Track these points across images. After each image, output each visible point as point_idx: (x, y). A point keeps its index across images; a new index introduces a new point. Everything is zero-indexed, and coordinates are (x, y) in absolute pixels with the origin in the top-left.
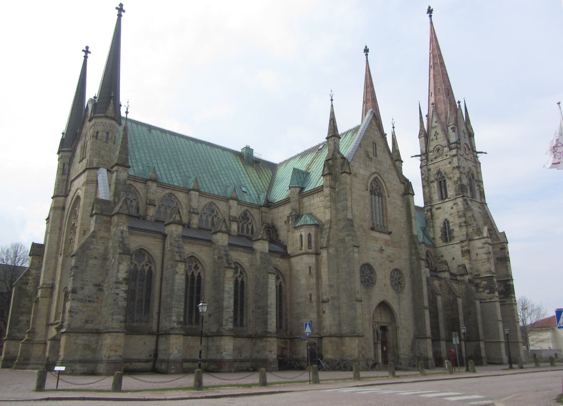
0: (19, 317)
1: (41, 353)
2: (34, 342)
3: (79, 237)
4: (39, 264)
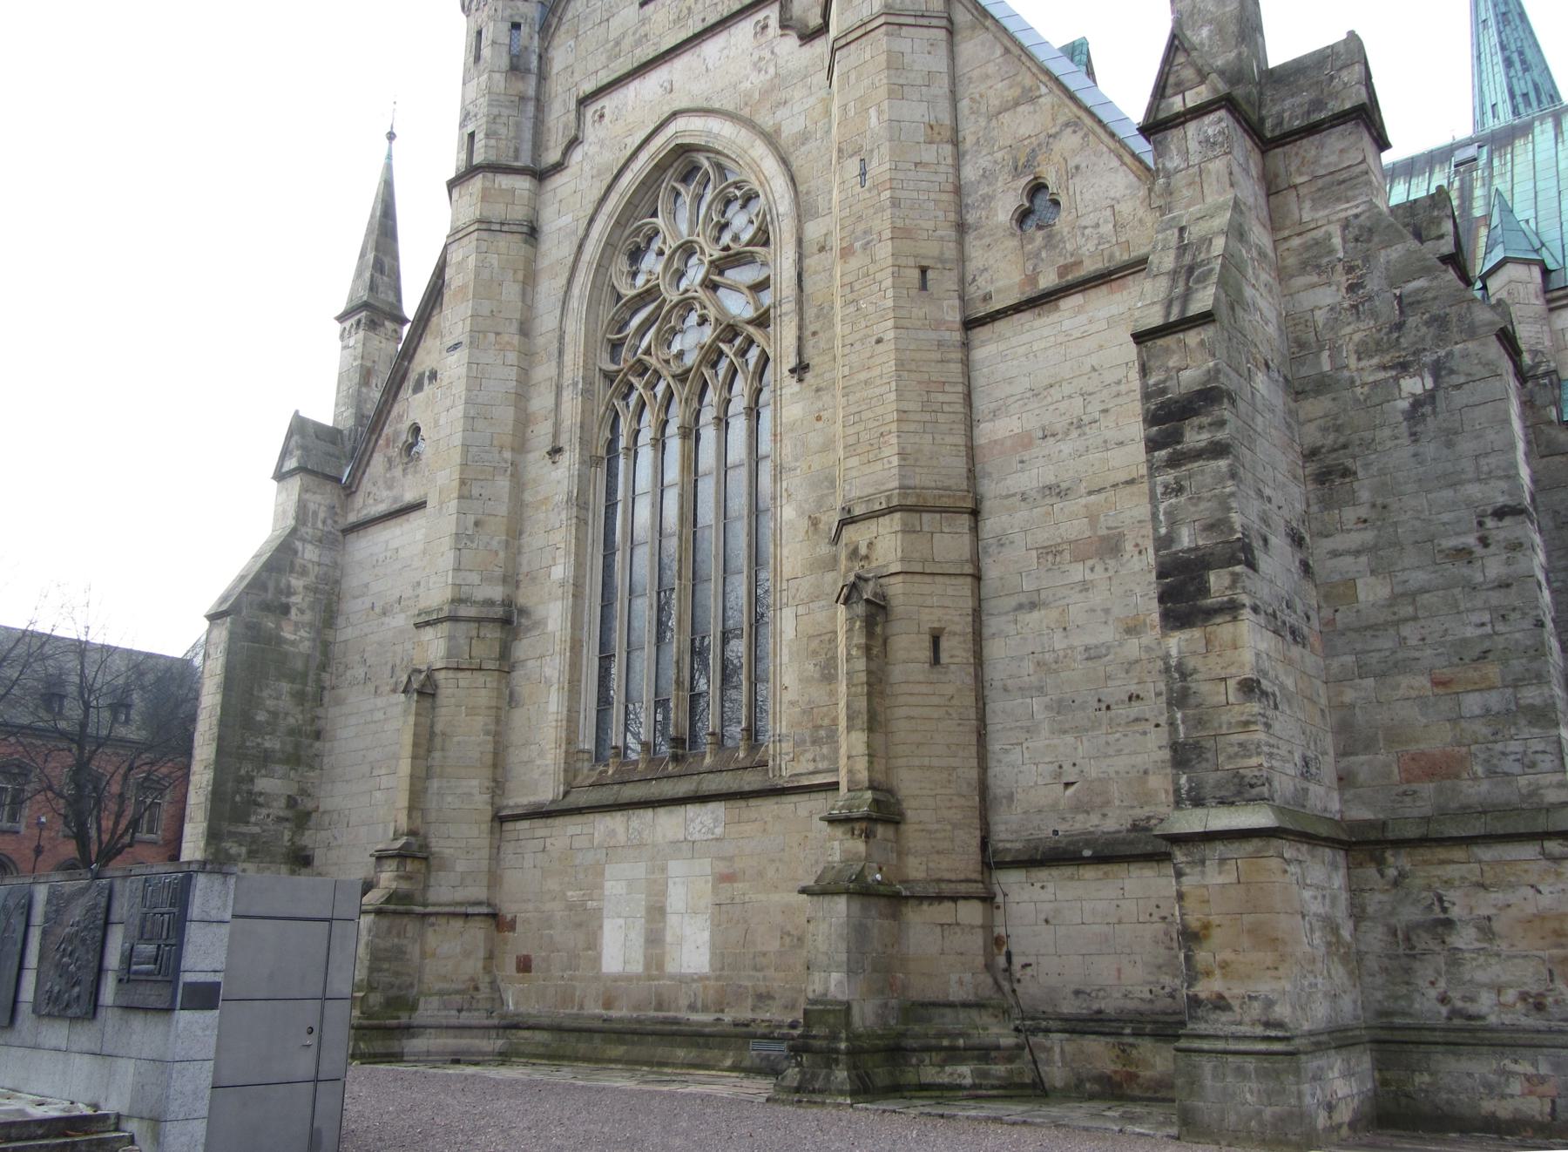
0: (252, 780)
1: (473, 966)
2: (430, 909)
3: (895, 298)
4: (329, 522)
